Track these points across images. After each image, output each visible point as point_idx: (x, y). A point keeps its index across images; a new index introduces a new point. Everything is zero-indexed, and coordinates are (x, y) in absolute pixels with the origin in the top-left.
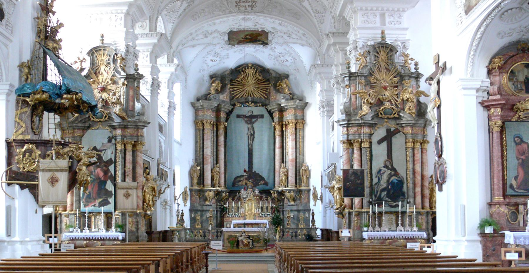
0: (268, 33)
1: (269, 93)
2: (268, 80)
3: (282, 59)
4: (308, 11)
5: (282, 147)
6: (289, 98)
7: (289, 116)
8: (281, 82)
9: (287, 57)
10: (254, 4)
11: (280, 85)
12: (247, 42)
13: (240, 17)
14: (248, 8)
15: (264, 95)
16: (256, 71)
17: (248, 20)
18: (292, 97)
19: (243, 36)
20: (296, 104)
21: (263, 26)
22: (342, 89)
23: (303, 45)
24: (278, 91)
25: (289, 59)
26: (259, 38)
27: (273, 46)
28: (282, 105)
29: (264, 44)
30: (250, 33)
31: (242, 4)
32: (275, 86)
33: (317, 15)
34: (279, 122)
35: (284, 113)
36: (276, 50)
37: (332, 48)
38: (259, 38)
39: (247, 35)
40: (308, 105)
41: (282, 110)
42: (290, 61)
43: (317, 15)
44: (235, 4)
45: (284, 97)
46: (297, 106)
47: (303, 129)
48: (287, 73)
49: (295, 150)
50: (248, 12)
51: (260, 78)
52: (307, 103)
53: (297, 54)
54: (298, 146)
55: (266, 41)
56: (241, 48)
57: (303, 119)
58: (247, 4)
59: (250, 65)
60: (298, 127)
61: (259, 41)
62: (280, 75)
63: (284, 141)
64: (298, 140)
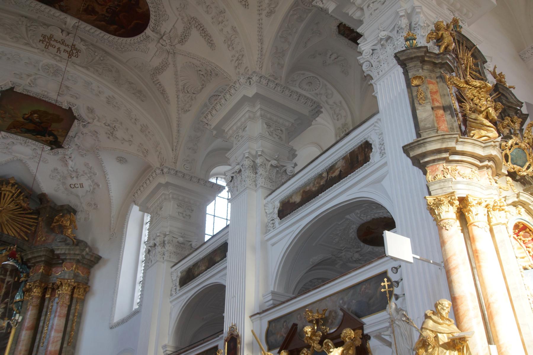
0: (75, 118)
1: (35, 233)
2: (37, 212)
3: (74, 181)
4: (163, 92)
5: (36, 329)
6: (72, 243)
7: (63, 273)
8: (62, 216)
9: (83, 180)
10: (74, 52)
11: (58, 221)
12: (28, 131)
13: (47, 60)
14: (62, 52)
15: (22, 234)
16: (20, 193)
17: (56, 72)
18: (78, 243)
19: (27, 111)
20: (84, 253)
21: (72, 100)
22: (261, 181)
23: (121, 160)
24: (52, 230)
25: (87, 184)
26: (54, 126)
27: (68, 152)
28: (57, 252)
29: (56, 144)
30: (43, 109)
31: (53, 43)
32: (50, 221)
33: (181, 95)
34: (41, 282)
35: (54, 269)
36: (71, 163)
37: (246, 108)
38: (54, 126)
39: (35, 112)
40: (101, 262)
41: (53, 261)
42: (86, 187)
43: (181, 95)
44: (42, 38)
45: (64, 241)
46: (83, 257)
47: (83, 302)
48: (75, 208)
49: (61, 335)
50: (60, 57)
51: (25, 205)
52: (99, 258)
53: (104, 174)
54: (68, 329)
55: (60, 139)
56: (10, 141)
57: (87, 283)
58: (63, 48)
59: (12, 182)
60: (75, 296)
61: (51, 134)
62: (62, 206)
63: (43, 318)
64: (71, 317)
